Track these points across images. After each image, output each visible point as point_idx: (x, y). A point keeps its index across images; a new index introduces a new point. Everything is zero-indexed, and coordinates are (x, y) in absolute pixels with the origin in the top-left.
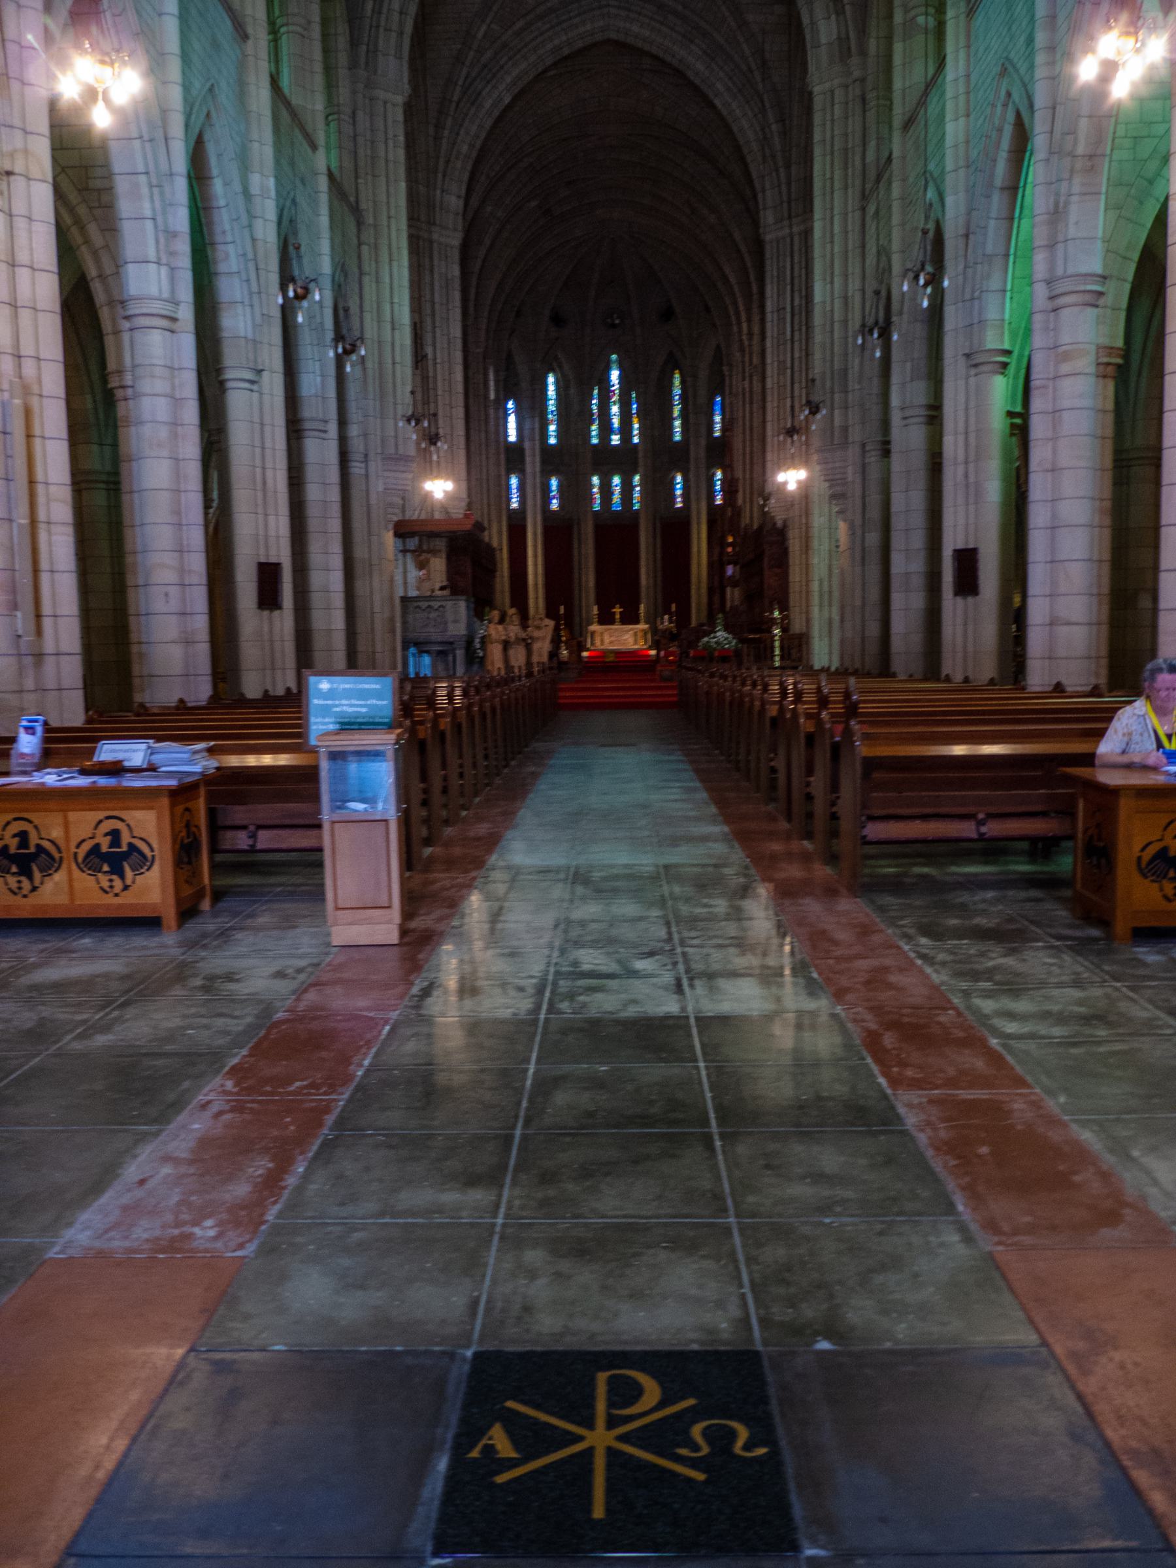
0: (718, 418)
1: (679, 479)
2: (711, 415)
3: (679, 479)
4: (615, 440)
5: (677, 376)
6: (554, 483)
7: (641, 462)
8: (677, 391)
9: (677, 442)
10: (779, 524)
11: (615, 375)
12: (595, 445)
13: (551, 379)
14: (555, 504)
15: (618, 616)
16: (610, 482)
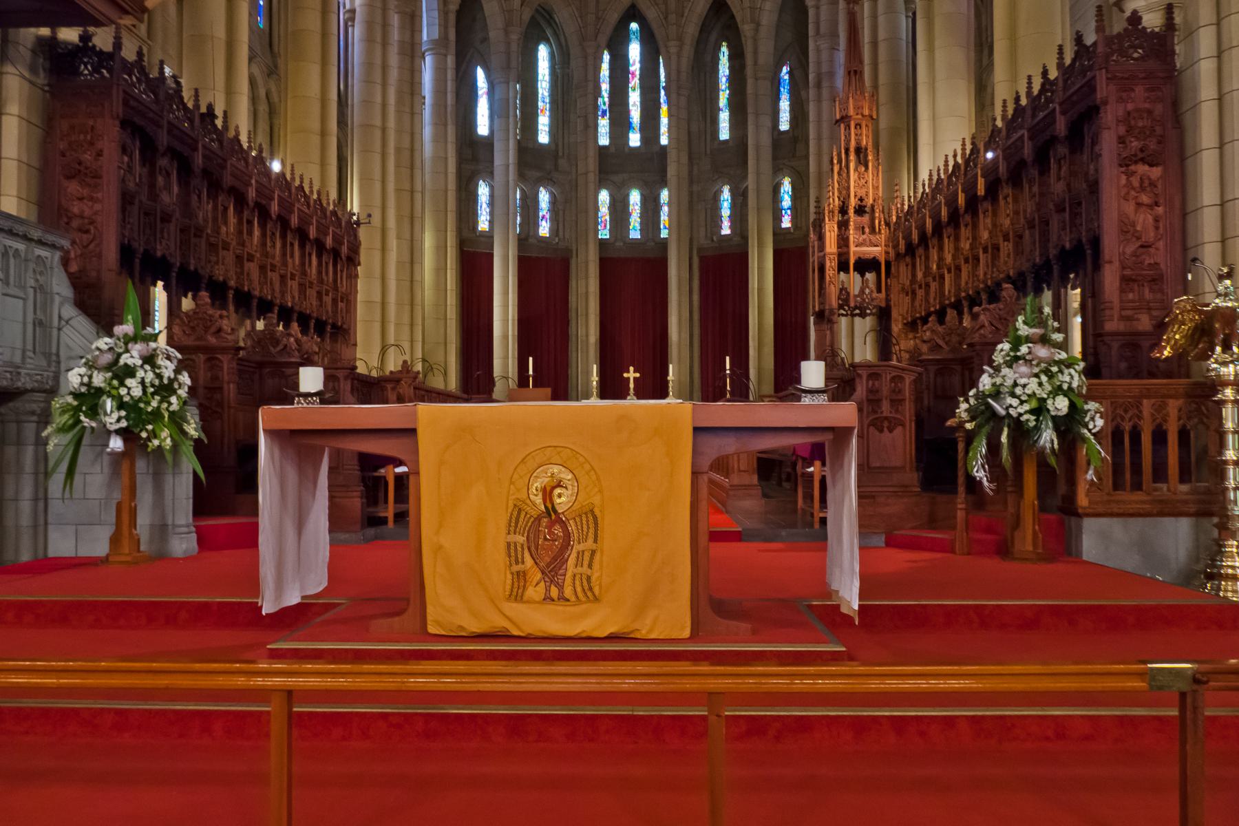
0: (785, 105)
1: (726, 194)
2: (777, 99)
3: (726, 194)
4: (635, 140)
5: (724, 49)
6: (544, 197)
7: (671, 171)
8: (724, 69)
9: (726, 141)
10: (1152, 21)
11: (634, 51)
12: (604, 147)
13: (543, 52)
14: (544, 229)
15: (632, 385)
16: (627, 196)
